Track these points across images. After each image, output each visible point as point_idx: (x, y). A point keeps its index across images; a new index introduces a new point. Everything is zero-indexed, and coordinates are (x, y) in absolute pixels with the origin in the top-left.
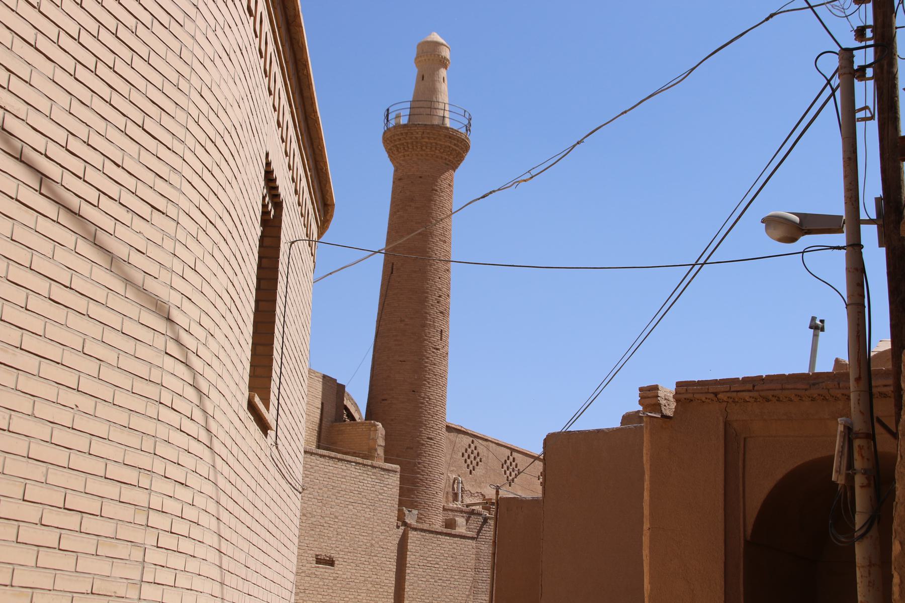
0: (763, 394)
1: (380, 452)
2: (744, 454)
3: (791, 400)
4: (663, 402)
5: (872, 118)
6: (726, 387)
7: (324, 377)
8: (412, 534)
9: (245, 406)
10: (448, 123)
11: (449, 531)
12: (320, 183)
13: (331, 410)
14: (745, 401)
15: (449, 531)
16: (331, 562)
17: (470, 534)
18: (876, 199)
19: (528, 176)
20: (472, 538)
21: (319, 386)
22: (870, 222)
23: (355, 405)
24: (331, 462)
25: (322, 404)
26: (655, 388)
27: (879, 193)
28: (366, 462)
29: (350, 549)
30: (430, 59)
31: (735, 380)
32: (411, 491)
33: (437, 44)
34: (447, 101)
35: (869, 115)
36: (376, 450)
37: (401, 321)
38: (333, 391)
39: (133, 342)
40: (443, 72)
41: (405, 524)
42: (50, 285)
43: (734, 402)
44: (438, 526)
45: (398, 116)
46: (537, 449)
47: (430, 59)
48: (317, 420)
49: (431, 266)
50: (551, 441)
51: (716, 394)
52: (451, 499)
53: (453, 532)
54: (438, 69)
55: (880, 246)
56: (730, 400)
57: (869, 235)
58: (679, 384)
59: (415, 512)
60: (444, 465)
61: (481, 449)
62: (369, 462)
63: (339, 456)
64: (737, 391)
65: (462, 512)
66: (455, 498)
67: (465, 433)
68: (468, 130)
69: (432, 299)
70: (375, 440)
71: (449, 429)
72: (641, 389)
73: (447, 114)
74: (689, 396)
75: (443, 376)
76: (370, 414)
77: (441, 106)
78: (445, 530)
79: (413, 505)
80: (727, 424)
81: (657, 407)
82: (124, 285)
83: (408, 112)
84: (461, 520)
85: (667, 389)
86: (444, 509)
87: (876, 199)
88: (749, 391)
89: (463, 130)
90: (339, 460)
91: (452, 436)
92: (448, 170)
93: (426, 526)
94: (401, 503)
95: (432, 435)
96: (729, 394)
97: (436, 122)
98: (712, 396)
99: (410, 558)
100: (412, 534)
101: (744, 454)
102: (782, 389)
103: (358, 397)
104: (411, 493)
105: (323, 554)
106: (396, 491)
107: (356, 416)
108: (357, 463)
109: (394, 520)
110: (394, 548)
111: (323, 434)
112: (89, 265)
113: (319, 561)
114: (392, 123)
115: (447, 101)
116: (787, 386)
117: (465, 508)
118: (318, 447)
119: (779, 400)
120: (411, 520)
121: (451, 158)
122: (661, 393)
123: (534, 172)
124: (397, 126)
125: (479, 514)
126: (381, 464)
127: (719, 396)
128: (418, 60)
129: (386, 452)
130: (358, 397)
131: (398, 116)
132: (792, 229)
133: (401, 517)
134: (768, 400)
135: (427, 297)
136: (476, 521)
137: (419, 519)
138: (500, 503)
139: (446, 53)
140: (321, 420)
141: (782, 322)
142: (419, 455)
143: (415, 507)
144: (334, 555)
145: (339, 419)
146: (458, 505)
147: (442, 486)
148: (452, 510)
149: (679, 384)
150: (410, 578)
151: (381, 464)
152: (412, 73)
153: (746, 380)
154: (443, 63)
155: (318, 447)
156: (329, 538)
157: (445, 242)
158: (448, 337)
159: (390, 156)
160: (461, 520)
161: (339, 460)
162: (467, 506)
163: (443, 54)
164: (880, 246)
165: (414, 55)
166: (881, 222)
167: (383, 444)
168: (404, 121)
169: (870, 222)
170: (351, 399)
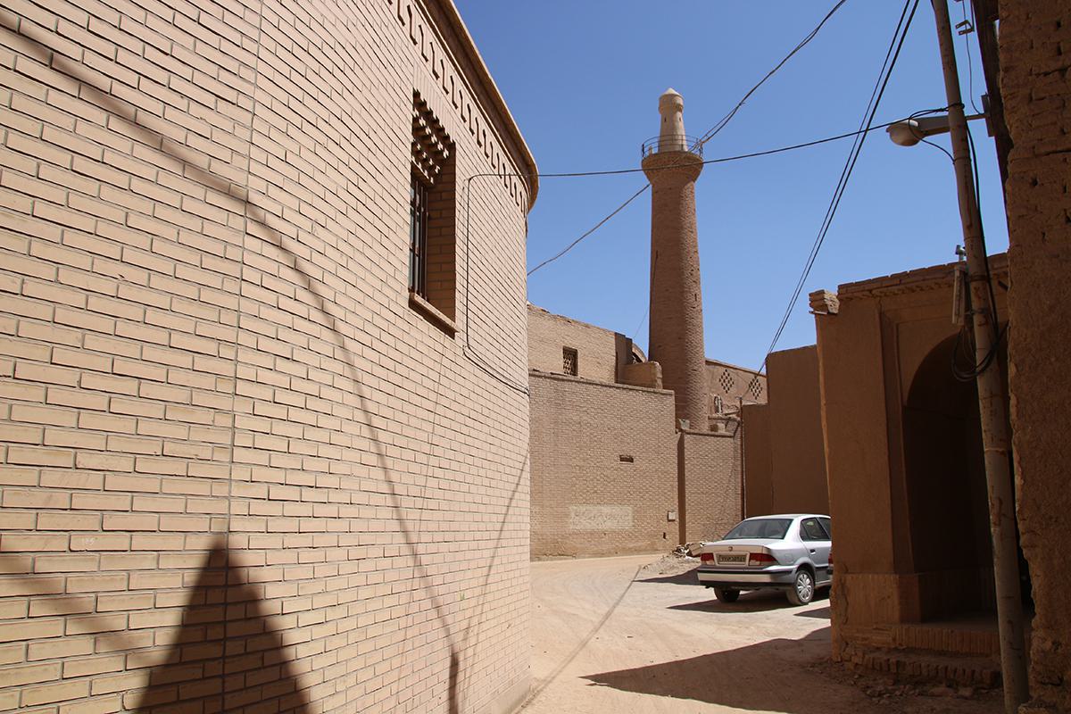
0: (908, 286)
1: (659, 382)
2: (897, 337)
3: (932, 289)
4: (829, 303)
5: (972, 30)
6: (878, 285)
7: (616, 334)
8: (687, 437)
9: (406, 306)
10: (686, 149)
11: (713, 433)
12: (516, 144)
13: (623, 358)
14: (895, 294)
15: (713, 433)
16: (631, 460)
17: (728, 434)
18: (982, 96)
19: (706, 138)
20: (730, 437)
21: (613, 340)
22: (979, 116)
23: (642, 353)
24: (625, 392)
25: (617, 353)
26: (822, 292)
27: (984, 91)
28: (649, 389)
29: (644, 450)
30: (669, 107)
31: (885, 278)
32: (684, 408)
33: (673, 96)
34: (684, 133)
35: (969, 27)
36: (656, 381)
37: (667, 290)
38: (624, 344)
39: (200, 221)
40: (679, 115)
41: (681, 430)
42: (73, 157)
43: (885, 295)
44: (705, 428)
45: (650, 149)
46: (757, 364)
47: (669, 107)
48: (614, 363)
49: (684, 249)
50: (772, 360)
51: (870, 291)
52: (713, 411)
53: (716, 433)
54: (675, 113)
55: (990, 136)
56: (883, 295)
57: (979, 131)
58: (840, 287)
59: (688, 421)
60: (706, 390)
61: (732, 375)
62: (652, 390)
63: (630, 387)
64: (887, 286)
65: (721, 419)
66: (717, 411)
67: (720, 365)
68: (701, 152)
69: (687, 273)
70: (655, 374)
71: (708, 363)
72: (810, 295)
73: (685, 143)
74: (849, 295)
75: (700, 326)
76: (651, 357)
77: (680, 137)
78: (710, 433)
79: (686, 417)
80: (881, 315)
81: (824, 307)
82: (181, 166)
83: (657, 144)
84: (721, 425)
85: (832, 293)
86: (709, 418)
87: (982, 96)
88: (896, 285)
89: (698, 153)
90: (631, 389)
91: (711, 367)
92: (688, 182)
93: (696, 431)
94: (677, 416)
95: (696, 368)
96: (881, 290)
97: (678, 149)
98: (867, 293)
99: (687, 453)
100: (687, 437)
101: (897, 337)
102: (924, 280)
103: (642, 345)
104: (684, 409)
105: (625, 454)
106: (673, 408)
107: (643, 360)
108: (643, 391)
109: (673, 428)
110: (676, 448)
111: (619, 374)
112: (130, 143)
113: (622, 459)
114: (647, 154)
115: (684, 133)
116: (927, 277)
117: (724, 417)
118: (617, 382)
119: (922, 290)
120: (685, 427)
121: (690, 173)
122: (826, 296)
123: (709, 135)
124: (651, 155)
125: (734, 420)
126: (661, 390)
127: (874, 292)
128: (661, 109)
129: (663, 382)
130: (642, 345)
131: (650, 149)
132: (912, 132)
133: (678, 426)
134: (913, 291)
135: (683, 272)
136: (732, 426)
137: (691, 427)
138: (743, 411)
139: (680, 101)
140: (617, 363)
141: (915, 220)
142: (688, 382)
143: (688, 418)
144: (632, 454)
145: (629, 362)
146: (720, 415)
147: (706, 402)
148: (715, 419)
149: (840, 287)
150: (688, 465)
151: (661, 390)
152: (657, 118)
153: (894, 276)
154: (678, 108)
155: (617, 382)
156: (628, 444)
157: (692, 232)
158: (700, 298)
159: (648, 177)
160: (721, 425)
161: (631, 389)
162: (726, 415)
163: (678, 102)
164: (990, 136)
165: (658, 106)
166: (988, 115)
167: (661, 377)
168: (655, 151)
169: (979, 116)
170: (637, 348)
